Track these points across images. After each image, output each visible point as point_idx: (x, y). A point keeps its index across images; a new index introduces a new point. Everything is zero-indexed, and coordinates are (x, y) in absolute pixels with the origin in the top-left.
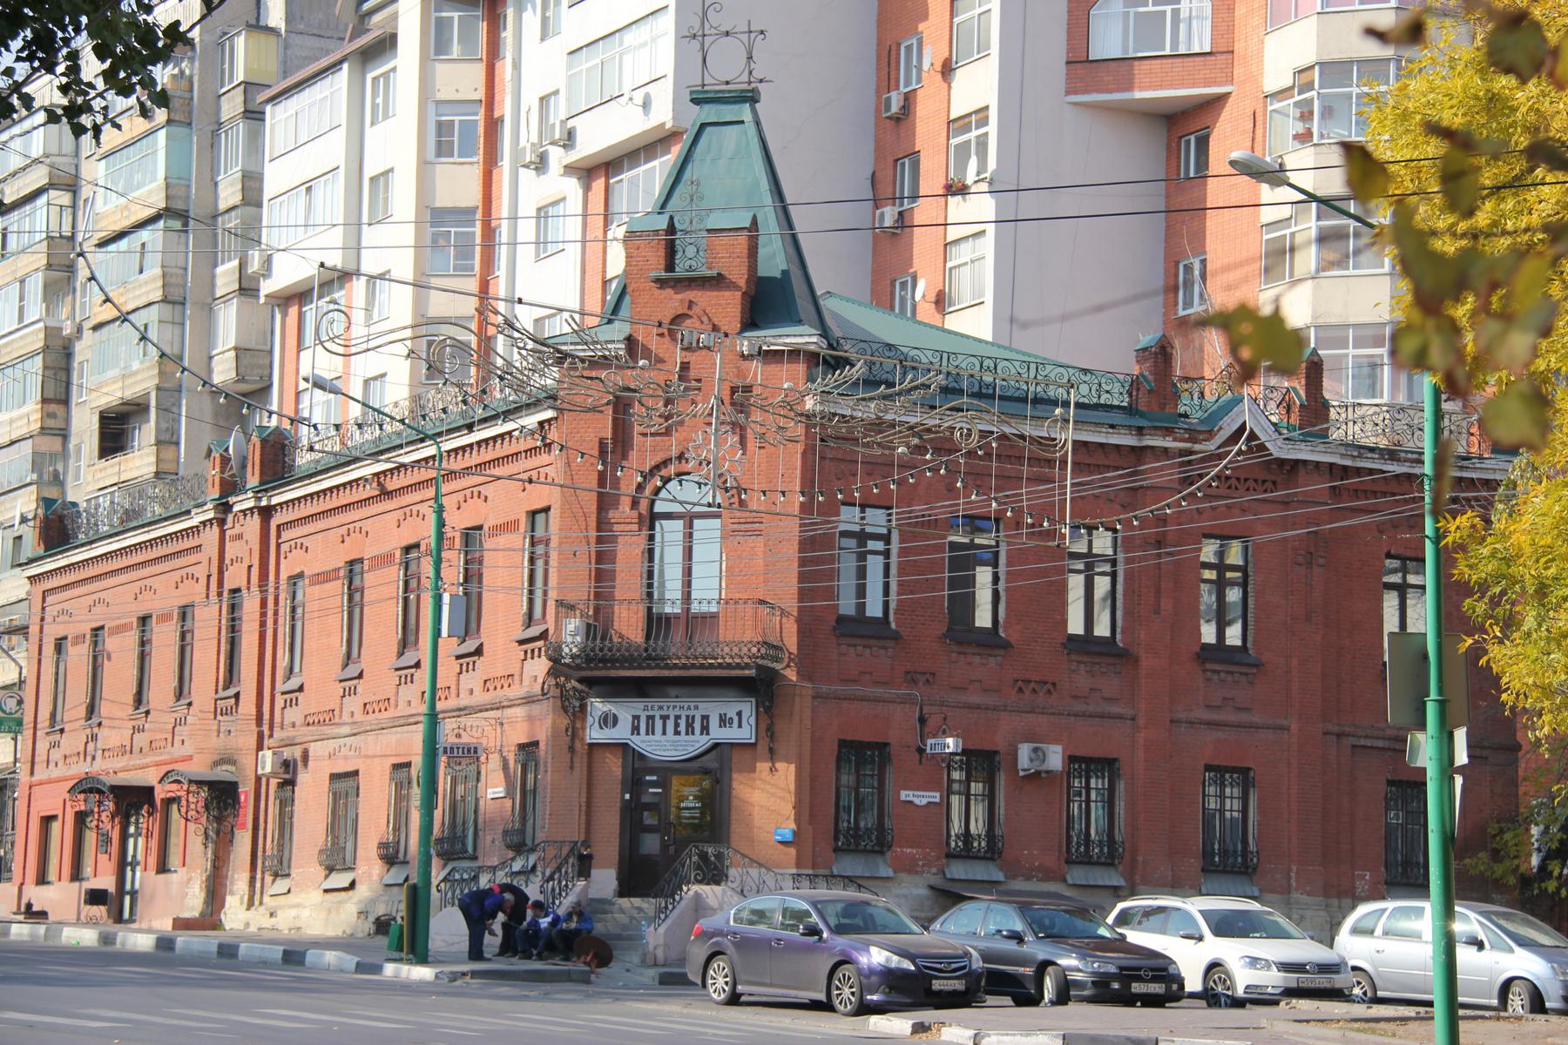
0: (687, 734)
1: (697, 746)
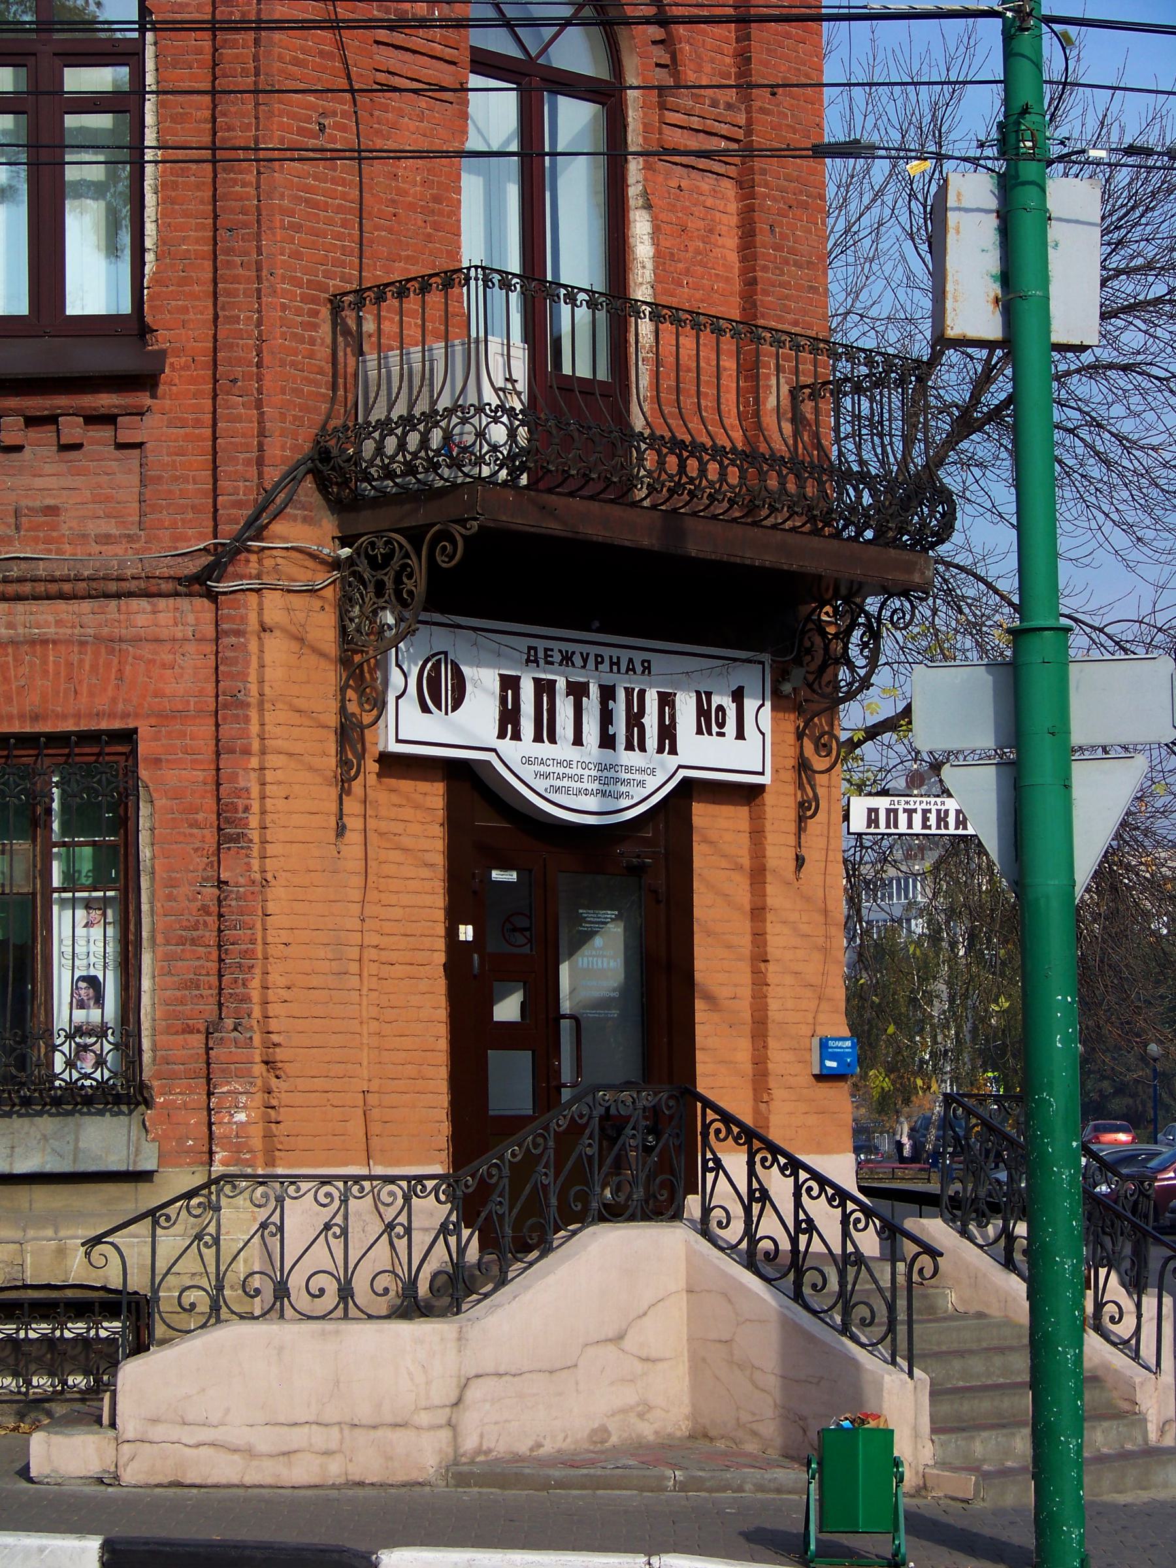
0: (629, 747)
1: (652, 783)
